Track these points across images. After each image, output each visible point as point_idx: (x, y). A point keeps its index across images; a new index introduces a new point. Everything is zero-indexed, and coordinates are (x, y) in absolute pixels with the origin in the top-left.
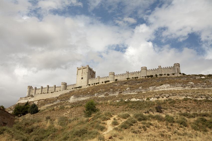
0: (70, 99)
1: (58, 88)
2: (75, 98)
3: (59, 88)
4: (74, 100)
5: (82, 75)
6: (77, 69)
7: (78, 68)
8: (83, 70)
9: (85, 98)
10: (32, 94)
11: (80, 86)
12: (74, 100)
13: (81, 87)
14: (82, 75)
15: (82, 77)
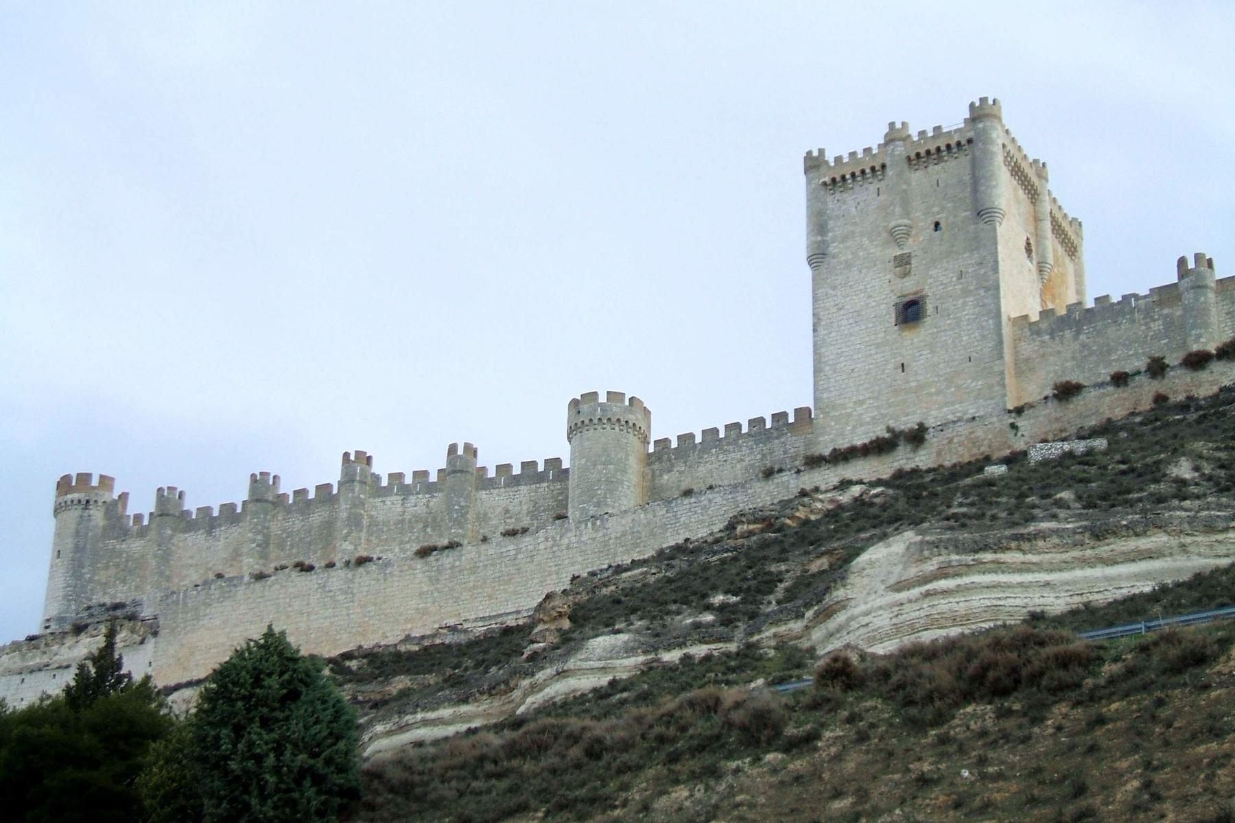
0: (842, 605)
1: (516, 481)
2: (942, 573)
3: (524, 489)
4: (943, 605)
5: (903, 262)
6: (796, 186)
7: (813, 163)
8: (918, 178)
9: (1149, 555)
10: (121, 594)
11: (907, 423)
12: (943, 605)
13: (917, 437)
14: (903, 262)
15: (909, 287)
